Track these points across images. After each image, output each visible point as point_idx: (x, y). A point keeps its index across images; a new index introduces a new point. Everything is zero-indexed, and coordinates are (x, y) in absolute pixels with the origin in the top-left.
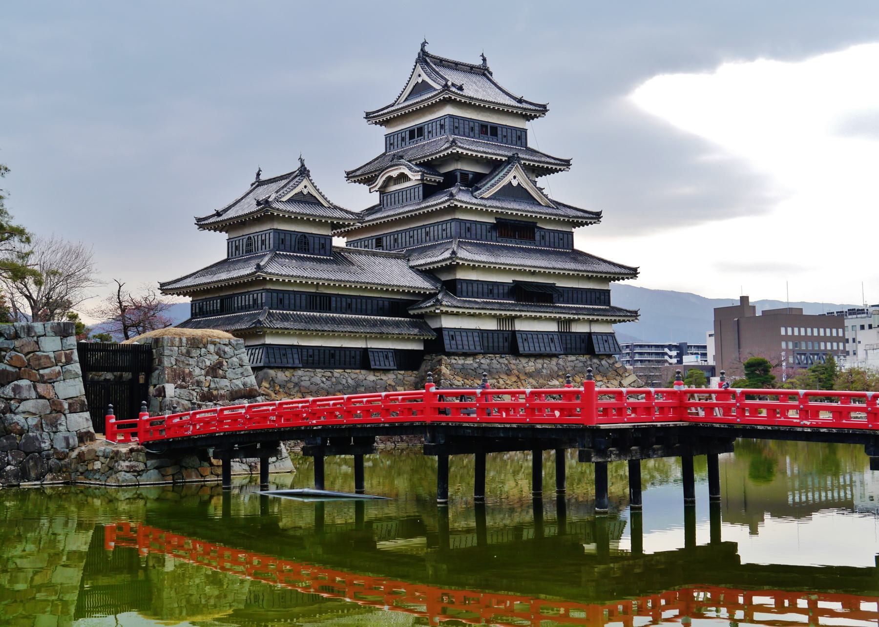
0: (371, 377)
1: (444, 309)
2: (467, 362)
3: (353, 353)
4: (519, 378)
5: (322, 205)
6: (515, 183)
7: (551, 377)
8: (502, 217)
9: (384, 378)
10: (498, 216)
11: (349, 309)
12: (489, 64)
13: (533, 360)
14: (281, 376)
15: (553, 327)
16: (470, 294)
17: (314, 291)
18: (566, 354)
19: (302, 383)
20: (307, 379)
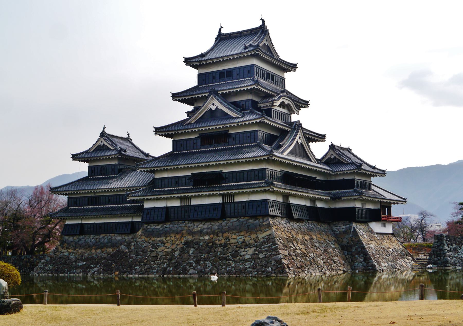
0: (119, 238)
1: (132, 198)
2: (157, 227)
3: (111, 225)
4: (183, 234)
5: (110, 149)
6: (213, 108)
7: (207, 234)
8: (203, 132)
9: (126, 238)
10: (201, 133)
11: (110, 202)
12: (266, 24)
13: (203, 223)
14: (71, 239)
15: (218, 200)
16: (163, 186)
17: (90, 195)
18: (231, 218)
19: (80, 243)
20: (83, 240)
